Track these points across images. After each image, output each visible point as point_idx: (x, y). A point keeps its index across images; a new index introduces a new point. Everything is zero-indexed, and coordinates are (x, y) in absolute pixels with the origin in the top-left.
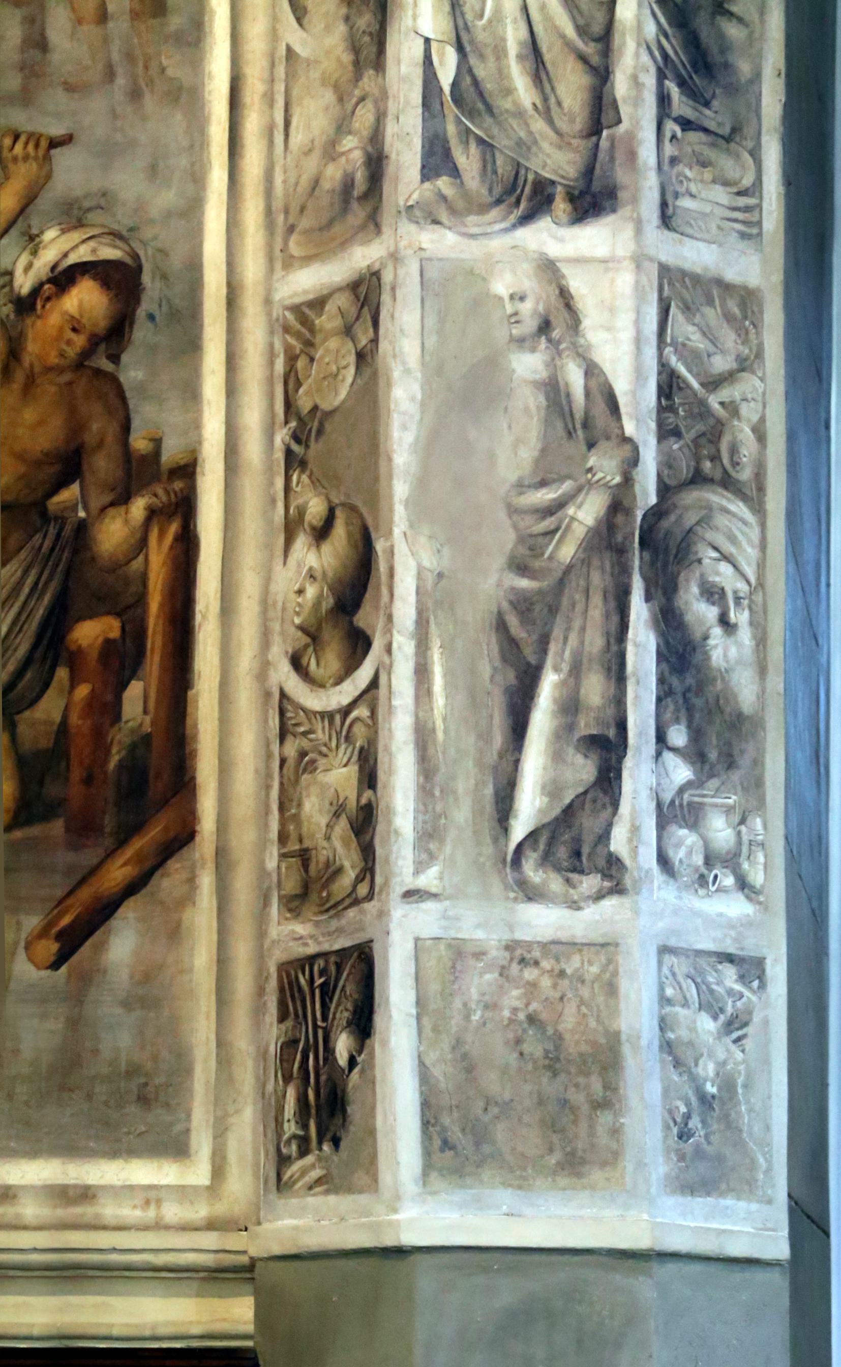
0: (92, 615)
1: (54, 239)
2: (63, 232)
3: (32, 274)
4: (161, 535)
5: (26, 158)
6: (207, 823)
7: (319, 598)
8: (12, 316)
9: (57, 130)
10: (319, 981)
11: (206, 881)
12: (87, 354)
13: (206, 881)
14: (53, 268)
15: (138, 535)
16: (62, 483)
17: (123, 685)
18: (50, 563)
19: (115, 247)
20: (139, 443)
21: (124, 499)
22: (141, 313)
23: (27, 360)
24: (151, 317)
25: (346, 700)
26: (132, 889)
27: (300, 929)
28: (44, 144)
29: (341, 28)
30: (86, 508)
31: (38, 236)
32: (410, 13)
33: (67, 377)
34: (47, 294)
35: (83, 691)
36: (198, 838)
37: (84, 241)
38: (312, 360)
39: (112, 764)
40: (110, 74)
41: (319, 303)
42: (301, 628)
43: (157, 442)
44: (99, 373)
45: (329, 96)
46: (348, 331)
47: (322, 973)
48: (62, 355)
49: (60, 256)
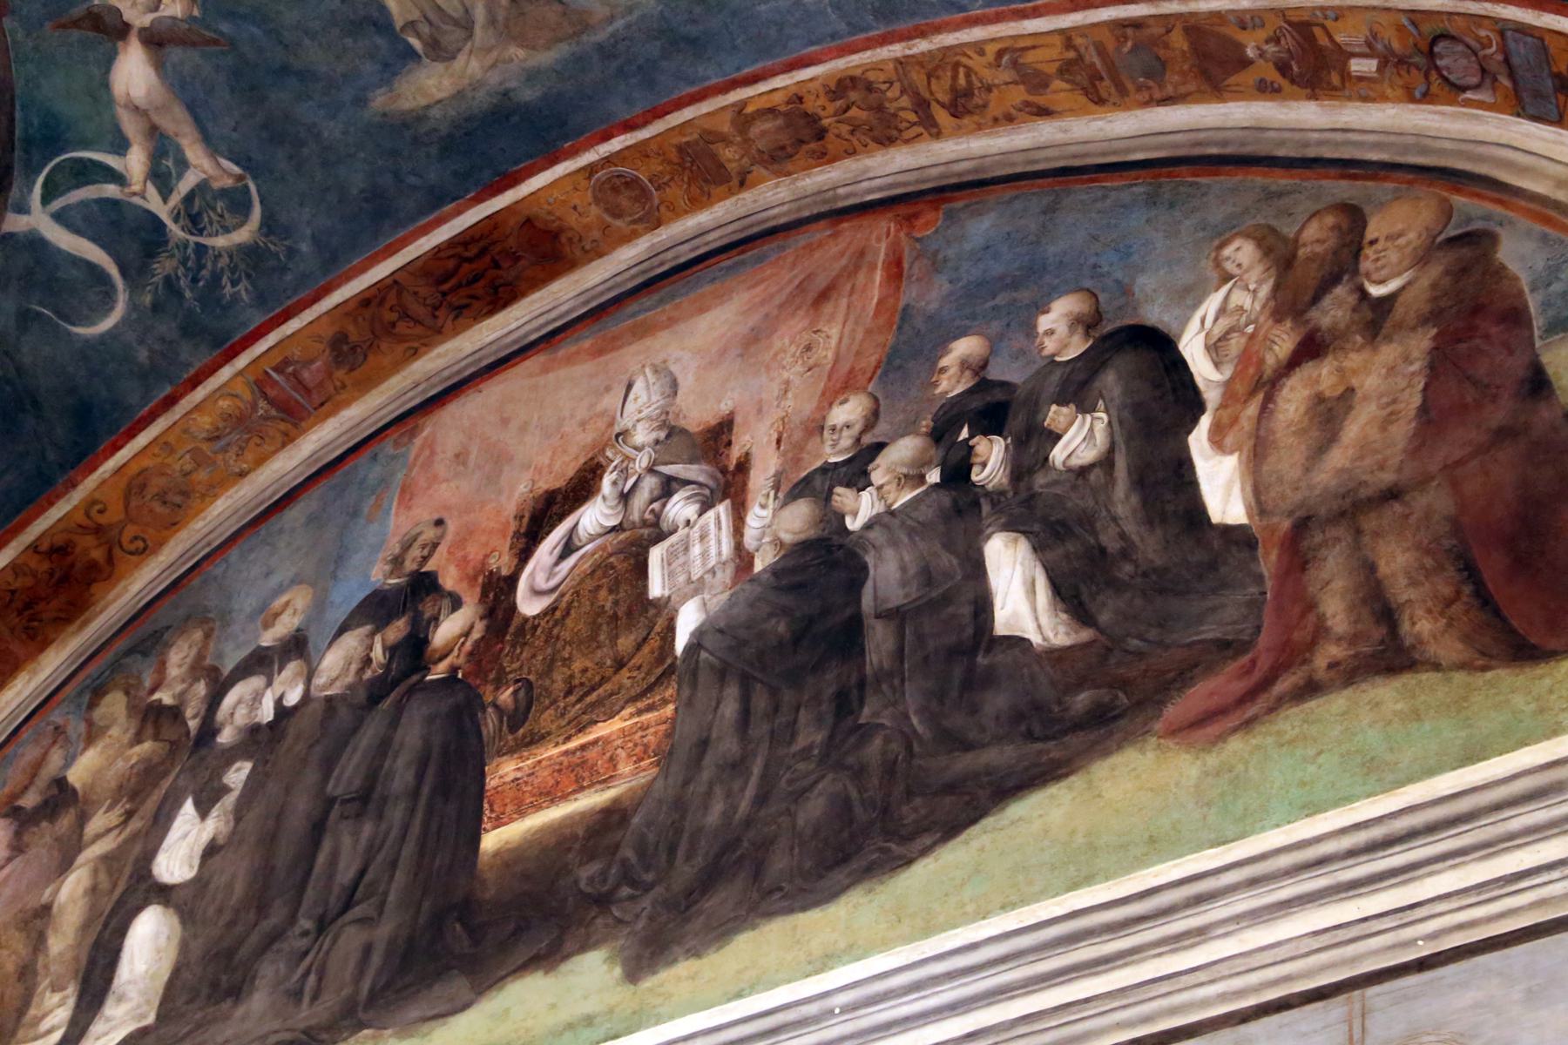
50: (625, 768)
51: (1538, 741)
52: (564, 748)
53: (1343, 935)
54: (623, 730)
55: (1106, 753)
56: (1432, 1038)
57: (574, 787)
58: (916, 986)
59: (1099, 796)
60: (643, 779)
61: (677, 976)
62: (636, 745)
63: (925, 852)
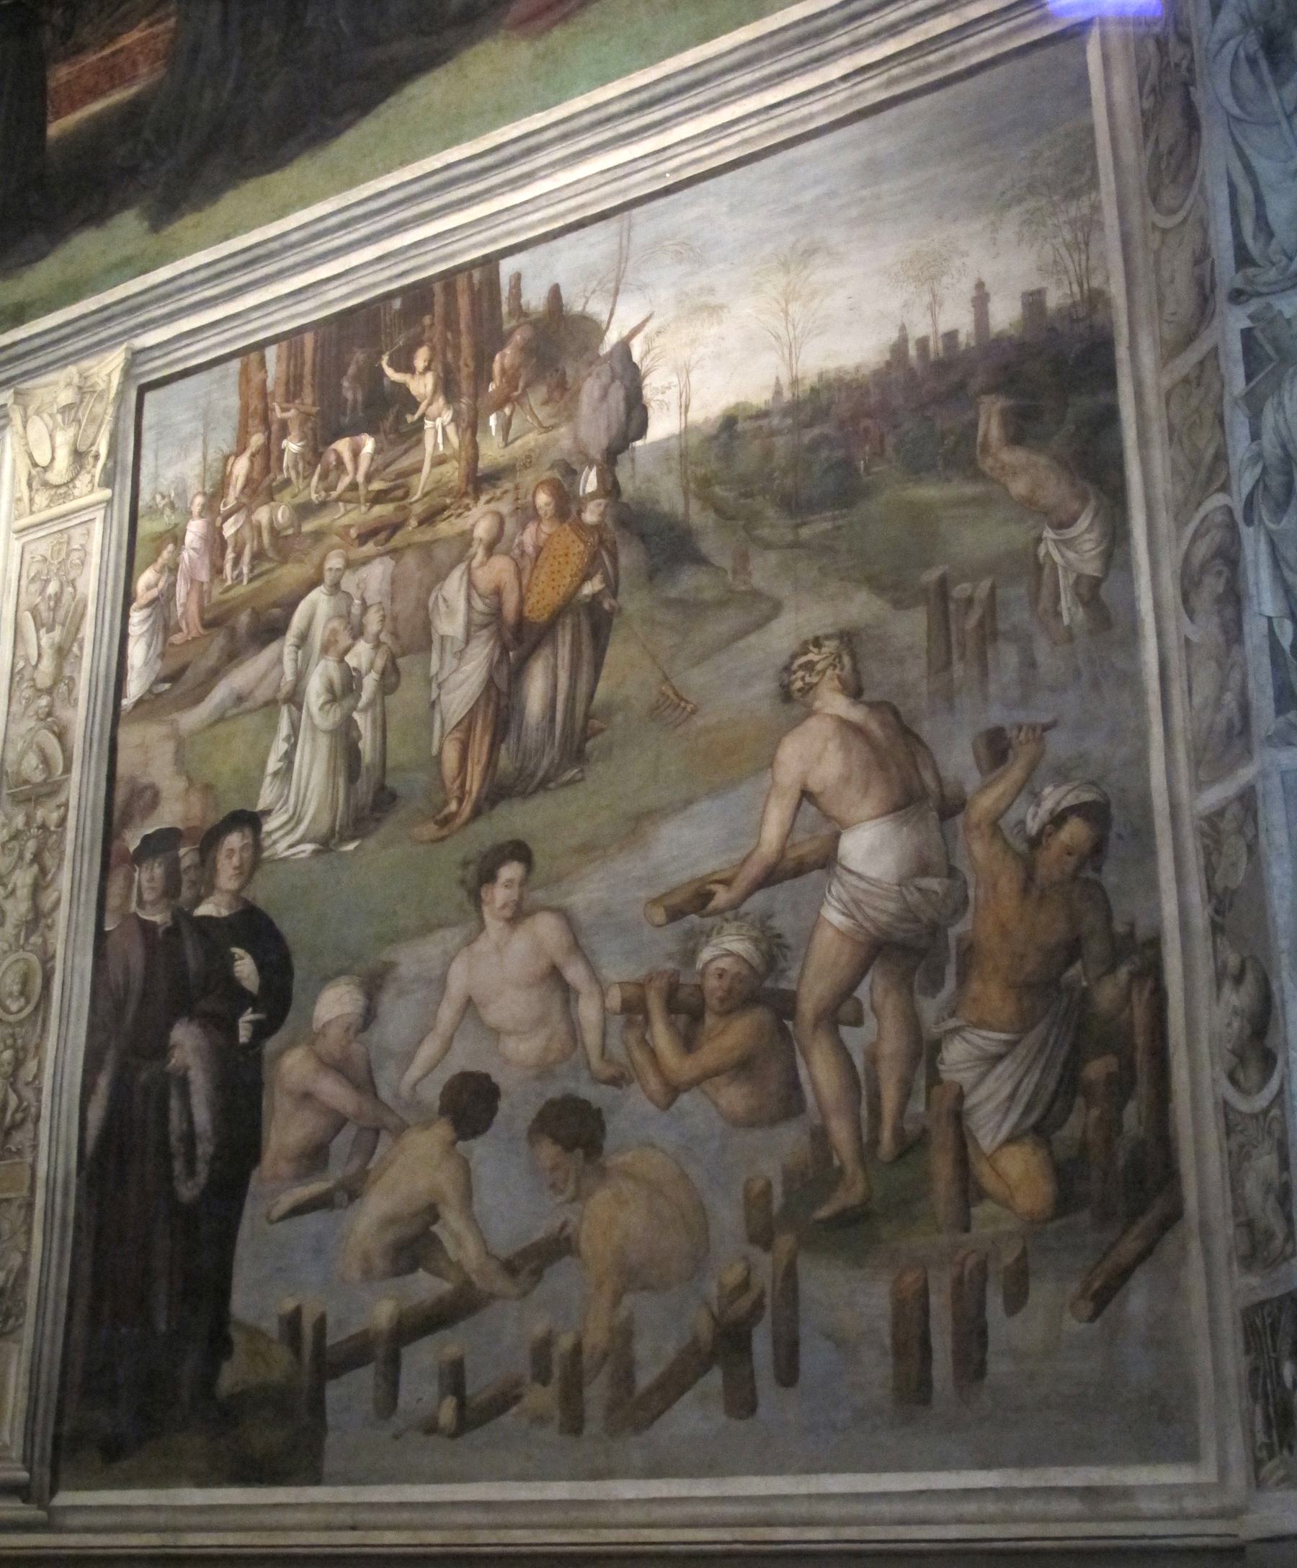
2: (1056, 787)
3: (1037, 820)
5: (1028, 741)
7: (1242, 1028)
9: (1046, 718)
10: (1269, 1321)
12: (1080, 867)
13: (1195, 1247)
14: (1051, 813)
16: (1069, 963)
17: (1120, 1108)
20: (1119, 928)
21: (1112, 968)
22: (1112, 835)
24: (1120, 836)
25: (1265, 1104)
26: (1142, 1257)
27: (1254, 1281)
28: (1039, 732)
29: (1216, 620)
32: (1255, 601)
35: (1095, 1113)
37: (1069, 792)
38: (1220, 853)
39: (1121, 1163)
41: (1221, 813)
42: (1233, 1052)
43: (1132, 925)
44: (1088, 880)
45: (1213, 665)
46: (1240, 831)
47: (1269, 1315)
50: (143, 70)
51: (748, 23)
52: (99, 55)
53: (620, 172)
54: (140, 39)
55: (472, 43)
56: (671, 242)
57: (108, 86)
58: (344, 225)
59: (466, 76)
60: (156, 77)
61: (184, 226)
62: (150, 50)
63: (349, 125)
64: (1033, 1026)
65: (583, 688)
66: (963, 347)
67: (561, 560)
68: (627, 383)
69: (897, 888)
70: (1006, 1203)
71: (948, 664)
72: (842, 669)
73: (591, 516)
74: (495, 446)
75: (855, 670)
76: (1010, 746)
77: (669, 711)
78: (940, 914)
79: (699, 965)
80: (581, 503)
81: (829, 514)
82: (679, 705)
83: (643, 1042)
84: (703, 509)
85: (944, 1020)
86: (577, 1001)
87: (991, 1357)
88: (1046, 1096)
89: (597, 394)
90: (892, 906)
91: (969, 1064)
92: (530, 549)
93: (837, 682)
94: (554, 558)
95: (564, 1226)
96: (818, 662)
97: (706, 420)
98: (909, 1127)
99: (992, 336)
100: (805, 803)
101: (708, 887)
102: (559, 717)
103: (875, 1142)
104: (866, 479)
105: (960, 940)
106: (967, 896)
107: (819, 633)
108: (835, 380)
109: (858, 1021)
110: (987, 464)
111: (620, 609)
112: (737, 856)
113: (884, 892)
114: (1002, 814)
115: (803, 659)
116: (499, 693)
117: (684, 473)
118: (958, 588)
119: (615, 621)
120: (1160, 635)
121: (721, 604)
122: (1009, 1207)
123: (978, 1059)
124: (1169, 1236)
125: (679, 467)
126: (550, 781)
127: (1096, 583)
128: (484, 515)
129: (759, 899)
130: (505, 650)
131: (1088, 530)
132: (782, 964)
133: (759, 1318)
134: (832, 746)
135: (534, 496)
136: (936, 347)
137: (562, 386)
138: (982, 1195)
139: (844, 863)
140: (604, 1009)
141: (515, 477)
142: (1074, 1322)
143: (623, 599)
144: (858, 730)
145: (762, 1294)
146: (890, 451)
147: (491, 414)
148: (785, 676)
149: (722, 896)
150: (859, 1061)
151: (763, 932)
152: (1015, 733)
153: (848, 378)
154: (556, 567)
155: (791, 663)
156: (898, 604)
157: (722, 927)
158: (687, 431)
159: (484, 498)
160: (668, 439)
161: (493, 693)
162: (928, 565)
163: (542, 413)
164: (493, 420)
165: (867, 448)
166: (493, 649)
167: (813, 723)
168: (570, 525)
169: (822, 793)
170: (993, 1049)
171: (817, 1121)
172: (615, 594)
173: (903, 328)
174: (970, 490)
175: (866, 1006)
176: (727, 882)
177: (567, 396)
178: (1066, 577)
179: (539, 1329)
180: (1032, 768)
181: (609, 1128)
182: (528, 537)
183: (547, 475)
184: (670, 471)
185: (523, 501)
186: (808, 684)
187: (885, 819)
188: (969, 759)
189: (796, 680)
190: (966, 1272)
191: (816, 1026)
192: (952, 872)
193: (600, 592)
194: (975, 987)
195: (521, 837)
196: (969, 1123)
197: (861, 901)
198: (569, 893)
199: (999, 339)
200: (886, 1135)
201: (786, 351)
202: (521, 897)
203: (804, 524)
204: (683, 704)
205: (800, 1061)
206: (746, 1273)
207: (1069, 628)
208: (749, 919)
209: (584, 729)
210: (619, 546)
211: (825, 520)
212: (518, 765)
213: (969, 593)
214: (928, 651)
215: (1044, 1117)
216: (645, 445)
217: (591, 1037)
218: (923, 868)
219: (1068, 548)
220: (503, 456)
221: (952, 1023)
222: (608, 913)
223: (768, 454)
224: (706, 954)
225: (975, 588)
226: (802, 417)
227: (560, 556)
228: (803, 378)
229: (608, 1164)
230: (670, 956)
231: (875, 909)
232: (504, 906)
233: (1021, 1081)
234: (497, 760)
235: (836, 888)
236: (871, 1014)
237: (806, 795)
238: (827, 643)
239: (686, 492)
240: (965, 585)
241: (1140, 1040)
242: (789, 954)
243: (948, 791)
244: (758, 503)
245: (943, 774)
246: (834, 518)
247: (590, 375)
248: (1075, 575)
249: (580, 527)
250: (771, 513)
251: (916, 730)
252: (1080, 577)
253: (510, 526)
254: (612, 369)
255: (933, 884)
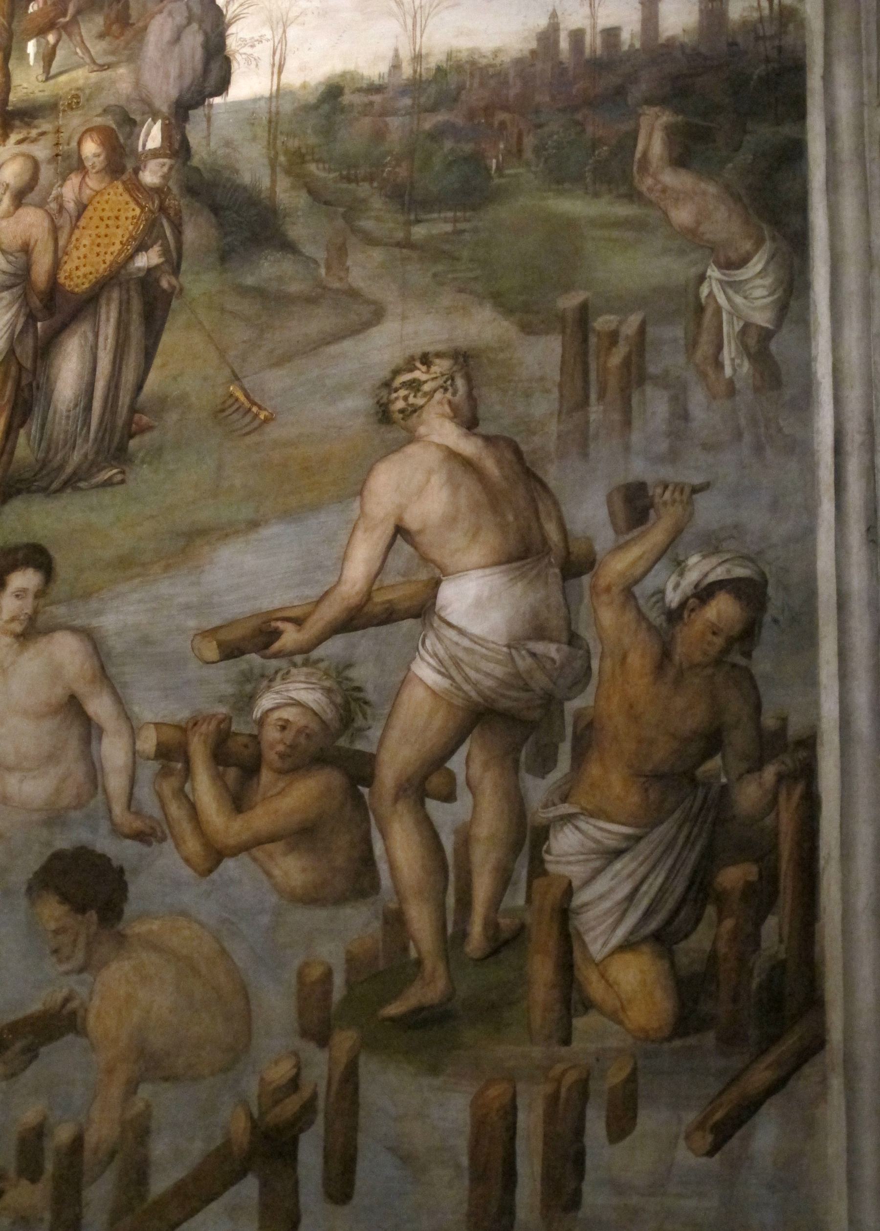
0: (734, 863)
1: (696, 563)
2: (704, 557)
3: (679, 591)
4: (789, 795)
5: (674, 501)
6: (836, 1034)
8: (665, 625)
9: (697, 480)
11: (836, 1083)
12: (726, 651)
13: (836, 1083)
14: (696, 586)
15: (770, 796)
16: (707, 755)
18: (700, 820)
19: (745, 567)
20: (769, 721)
21: (757, 765)
22: (767, 618)
23: (676, 658)
24: (776, 621)
28: (687, 491)
30: (727, 774)
31: (683, 561)
33: (709, 671)
34: (691, 607)
35: (729, 924)
36: (828, 1047)
37: (720, 564)
39: (754, 985)
40: (739, 435)
43: (784, 720)
44: (734, 666)
48: (705, 653)
49: (701, 577)
64: (661, 822)
65: (129, 377)
66: (625, 48)
67: (110, 222)
68: (208, 27)
69: (505, 649)
70: (614, 1016)
71: (584, 403)
72: (454, 394)
73: (151, 176)
74: (33, 78)
75: (471, 397)
76: (652, 505)
77: (235, 416)
78: (555, 683)
79: (257, 713)
80: (141, 160)
81: (450, 214)
82: (250, 409)
83: (180, 793)
84: (293, 187)
85: (554, 805)
86: (100, 739)
87: (586, 1188)
88: (670, 903)
89: (168, 35)
90: (499, 671)
91: (582, 857)
92: (71, 206)
93: (447, 409)
94: (102, 219)
95: (67, 1000)
96: (425, 382)
97: (304, 86)
98: (504, 922)
99: (662, 39)
100: (399, 540)
101: (274, 624)
102: (97, 405)
103: (463, 935)
104: (497, 181)
105: (578, 715)
106: (589, 668)
107: (430, 349)
108: (467, 62)
109: (449, 797)
110: (645, 184)
111: (181, 290)
112: (313, 592)
113: (490, 654)
114: (637, 581)
115: (407, 377)
116: (20, 367)
117: (271, 144)
118: (600, 320)
119: (175, 303)
120: (838, 401)
121: (312, 300)
122: (620, 1023)
123: (594, 852)
124: (807, 1069)
125: (266, 134)
126: (80, 480)
127: (766, 335)
128: (14, 157)
129: (335, 647)
130: (31, 318)
131: (761, 274)
132: (359, 722)
133: (311, 1123)
134: (437, 480)
135: (79, 143)
136: (593, 43)
137: (123, 20)
138: (588, 1005)
139: (443, 614)
140: (134, 753)
141: (57, 117)
142: (690, 1155)
143: (186, 279)
144: (467, 464)
145: (314, 1097)
146: (528, 154)
147: (29, 40)
148: (384, 393)
149: (290, 637)
150: (448, 842)
151: (339, 683)
152: (659, 491)
153: (484, 61)
154: (102, 231)
155: (393, 379)
156: (527, 329)
157: (288, 672)
158: (278, 94)
159: (14, 137)
160: (255, 100)
161: (13, 370)
162: (567, 288)
163: (97, 48)
164: (31, 47)
165: (502, 146)
166: (16, 315)
167: (412, 449)
168: (124, 183)
169: (420, 532)
170: (612, 843)
171: (393, 906)
172: (176, 270)
173: (554, 15)
174: (623, 210)
175: (461, 779)
176: (298, 622)
177: (129, 33)
178: (731, 323)
179: (30, 1115)
180: (677, 533)
181: (132, 890)
182: (70, 191)
183: (99, 121)
184: (254, 138)
185: (66, 147)
186: (412, 405)
187: (497, 569)
188: (603, 513)
189: (397, 398)
190: (563, 1090)
191: (396, 799)
192: (573, 639)
193: (157, 267)
194: (594, 770)
195: (44, 543)
196: (576, 923)
197: (461, 660)
198: (99, 613)
199: (670, 43)
200: (477, 928)
201: (409, 22)
202: (36, 612)
203: (418, 221)
204: (255, 409)
205: (376, 835)
206: (295, 1071)
207: (731, 382)
208: (322, 665)
209: (129, 422)
210: (186, 218)
211: (446, 220)
212: (41, 455)
213: (613, 326)
214: (561, 386)
215: (669, 922)
216: (226, 104)
217: (116, 783)
218: (539, 632)
219: (736, 292)
220: (43, 91)
221: (565, 809)
222: (146, 641)
223: (379, 135)
224: (266, 702)
225: (621, 323)
226: (423, 100)
227: (109, 218)
228: (428, 55)
229: (128, 932)
230: (221, 700)
231: (478, 670)
232: (13, 619)
233: (642, 882)
234: (14, 448)
235: (431, 642)
236: (466, 789)
237: (400, 531)
238: (437, 361)
239: (273, 164)
240: (608, 317)
241: (786, 848)
242: (369, 711)
243: (575, 548)
244: (364, 189)
245: (568, 527)
246: (455, 220)
247: (161, 12)
248: (741, 324)
249: (135, 188)
250: (377, 203)
251: (540, 473)
252: (747, 326)
253: (46, 173)
254: (189, 9)
255: (551, 650)
